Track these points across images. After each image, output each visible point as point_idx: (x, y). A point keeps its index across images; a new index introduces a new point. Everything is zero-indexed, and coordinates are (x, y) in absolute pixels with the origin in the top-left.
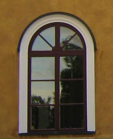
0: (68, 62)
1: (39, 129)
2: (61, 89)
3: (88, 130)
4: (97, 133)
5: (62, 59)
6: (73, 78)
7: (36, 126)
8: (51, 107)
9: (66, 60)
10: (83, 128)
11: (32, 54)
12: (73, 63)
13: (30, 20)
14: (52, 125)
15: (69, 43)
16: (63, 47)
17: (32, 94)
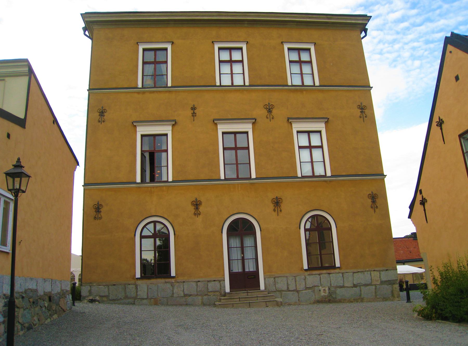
0: (160, 241)
1: (146, 276)
2: (157, 255)
3: (171, 276)
4: (176, 277)
5: (157, 239)
6: (163, 249)
7: (145, 274)
8: (153, 264)
9: (160, 240)
10: (169, 275)
11: (142, 237)
12: (163, 241)
13: (141, 220)
14: (153, 273)
15: (161, 231)
16: (158, 233)
17: (142, 258)
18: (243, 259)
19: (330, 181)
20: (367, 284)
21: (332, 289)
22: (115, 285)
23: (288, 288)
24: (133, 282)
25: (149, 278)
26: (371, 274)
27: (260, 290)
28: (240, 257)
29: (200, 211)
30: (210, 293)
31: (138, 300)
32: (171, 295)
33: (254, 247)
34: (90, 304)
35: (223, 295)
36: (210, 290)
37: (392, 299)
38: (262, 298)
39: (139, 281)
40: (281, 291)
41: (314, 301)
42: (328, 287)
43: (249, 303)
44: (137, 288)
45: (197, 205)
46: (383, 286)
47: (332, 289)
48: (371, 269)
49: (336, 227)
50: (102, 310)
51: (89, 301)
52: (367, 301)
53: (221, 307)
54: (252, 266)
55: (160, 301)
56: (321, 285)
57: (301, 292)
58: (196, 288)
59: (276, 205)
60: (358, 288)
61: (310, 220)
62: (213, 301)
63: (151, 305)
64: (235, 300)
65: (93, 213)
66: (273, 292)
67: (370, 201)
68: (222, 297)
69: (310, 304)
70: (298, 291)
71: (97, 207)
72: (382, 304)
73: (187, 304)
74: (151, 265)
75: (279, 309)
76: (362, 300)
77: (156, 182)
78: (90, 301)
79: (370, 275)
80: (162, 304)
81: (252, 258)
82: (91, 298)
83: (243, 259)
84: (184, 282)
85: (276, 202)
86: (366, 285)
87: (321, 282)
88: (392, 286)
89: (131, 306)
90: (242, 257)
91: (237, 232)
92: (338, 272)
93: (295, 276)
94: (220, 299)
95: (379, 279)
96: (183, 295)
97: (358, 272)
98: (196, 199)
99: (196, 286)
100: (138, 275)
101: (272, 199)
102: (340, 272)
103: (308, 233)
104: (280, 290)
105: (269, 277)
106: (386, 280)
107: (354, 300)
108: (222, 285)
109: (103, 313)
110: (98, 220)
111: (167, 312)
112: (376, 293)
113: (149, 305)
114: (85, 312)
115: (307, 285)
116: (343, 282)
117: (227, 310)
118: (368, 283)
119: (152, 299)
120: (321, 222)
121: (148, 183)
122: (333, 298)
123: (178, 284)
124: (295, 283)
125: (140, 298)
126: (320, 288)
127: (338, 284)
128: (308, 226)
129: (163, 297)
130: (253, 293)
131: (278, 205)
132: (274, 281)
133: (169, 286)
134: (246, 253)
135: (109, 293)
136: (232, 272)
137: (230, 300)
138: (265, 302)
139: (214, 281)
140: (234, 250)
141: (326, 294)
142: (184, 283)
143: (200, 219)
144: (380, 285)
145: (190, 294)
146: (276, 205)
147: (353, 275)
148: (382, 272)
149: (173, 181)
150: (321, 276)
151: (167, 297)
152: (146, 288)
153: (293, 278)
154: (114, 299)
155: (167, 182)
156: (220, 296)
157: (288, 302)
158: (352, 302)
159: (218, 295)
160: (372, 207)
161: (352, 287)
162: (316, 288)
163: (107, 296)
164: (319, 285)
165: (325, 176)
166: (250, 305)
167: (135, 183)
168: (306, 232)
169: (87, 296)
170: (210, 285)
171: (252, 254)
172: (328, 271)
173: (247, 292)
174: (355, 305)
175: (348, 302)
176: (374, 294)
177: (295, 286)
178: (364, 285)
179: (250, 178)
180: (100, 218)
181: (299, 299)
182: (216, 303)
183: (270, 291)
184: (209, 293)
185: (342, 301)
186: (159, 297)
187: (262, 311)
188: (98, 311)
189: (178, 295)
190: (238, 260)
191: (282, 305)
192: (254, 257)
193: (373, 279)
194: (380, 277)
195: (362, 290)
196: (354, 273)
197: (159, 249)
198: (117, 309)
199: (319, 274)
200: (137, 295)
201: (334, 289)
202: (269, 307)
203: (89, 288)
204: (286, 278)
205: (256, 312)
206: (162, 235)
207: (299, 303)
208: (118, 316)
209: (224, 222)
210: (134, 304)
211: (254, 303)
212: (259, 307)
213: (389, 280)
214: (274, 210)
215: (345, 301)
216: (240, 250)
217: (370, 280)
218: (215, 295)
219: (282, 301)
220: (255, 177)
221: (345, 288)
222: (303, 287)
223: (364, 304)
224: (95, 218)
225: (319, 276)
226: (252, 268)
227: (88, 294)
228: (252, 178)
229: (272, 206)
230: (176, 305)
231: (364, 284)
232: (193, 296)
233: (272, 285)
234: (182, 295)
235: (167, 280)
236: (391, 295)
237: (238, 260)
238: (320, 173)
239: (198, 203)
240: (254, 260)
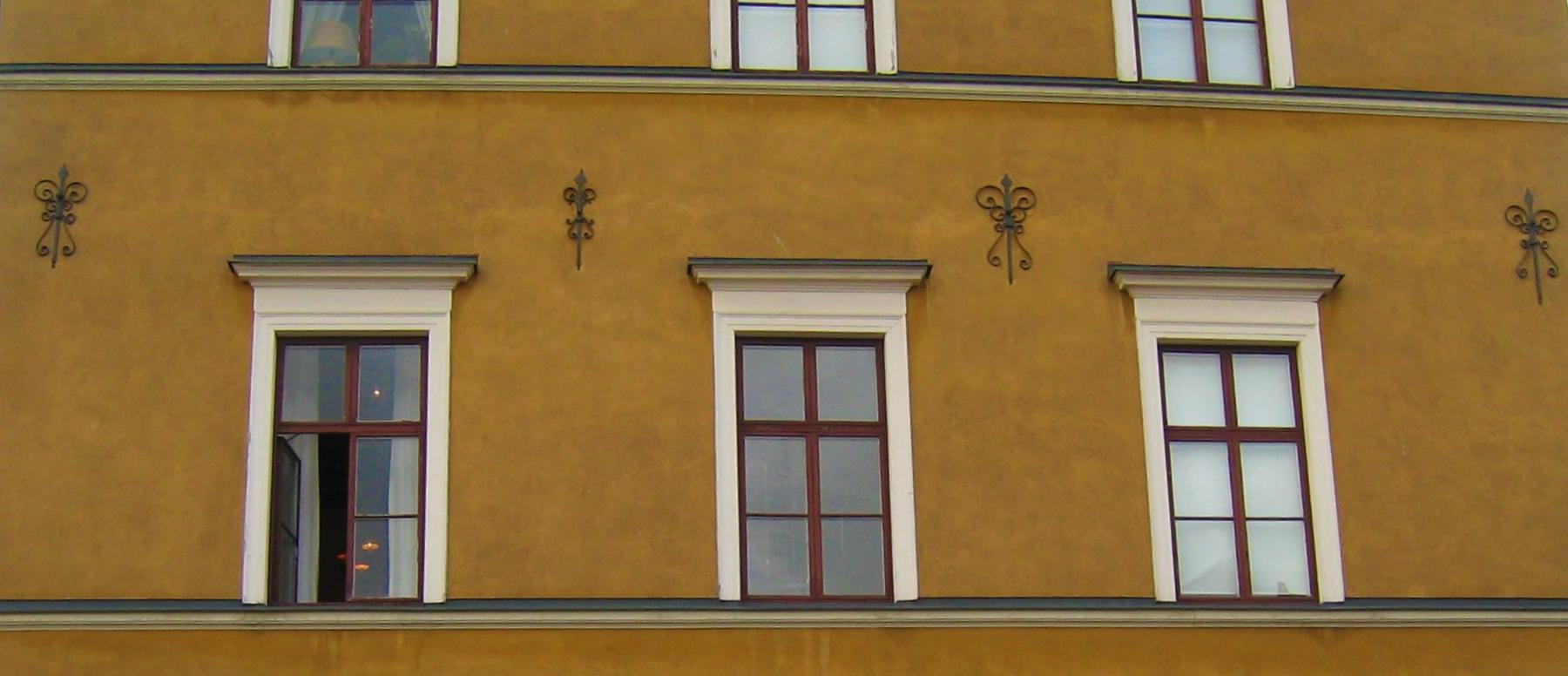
19: (1341, 631)
121: (307, 608)
149: (450, 605)
155: (416, 604)
165: (1310, 602)
179: (886, 600)
220: (915, 597)
228: (896, 600)
238: (1281, 585)
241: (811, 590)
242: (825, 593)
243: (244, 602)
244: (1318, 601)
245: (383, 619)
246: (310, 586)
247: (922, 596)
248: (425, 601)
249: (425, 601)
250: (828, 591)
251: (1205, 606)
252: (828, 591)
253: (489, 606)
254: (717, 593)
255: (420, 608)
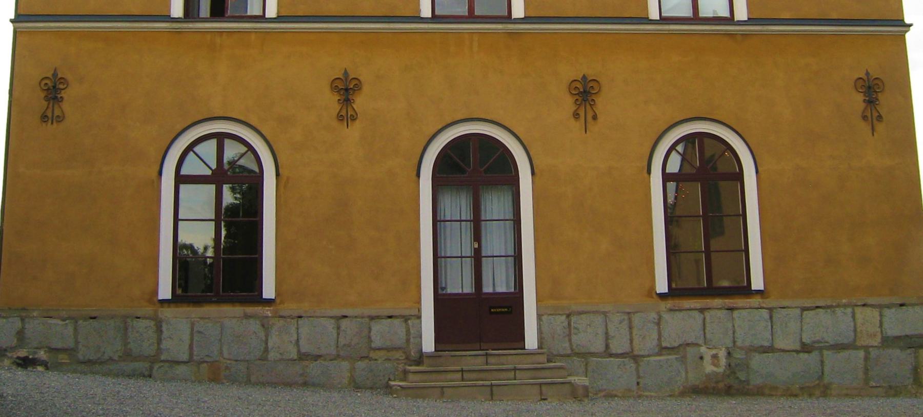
0: (235, 193)
1: (189, 294)
2: (224, 233)
3: (264, 297)
4: (278, 301)
5: (226, 188)
6: (243, 217)
7: (185, 290)
9: (233, 190)
10: (256, 293)
11: (181, 179)
12: (243, 194)
13: (179, 128)
14: (209, 288)
15: (238, 163)
16: (228, 170)
17: (179, 240)
18: (477, 257)
19: (745, 35)
20: (841, 344)
21: (739, 355)
22: (94, 318)
23: (607, 346)
24: (149, 310)
25: (197, 301)
26: (853, 316)
27: (524, 348)
28: (468, 251)
29: (354, 109)
30: (377, 351)
31: (162, 366)
32: (261, 354)
33: (512, 222)
34: (20, 373)
35: (415, 361)
36: (377, 342)
37: (914, 391)
38: (529, 374)
39: (167, 309)
40: (585, 355)
41: (681, 388)
42: (727, 348)
43: (489, 389)
44: (159, 330)
45: (347, 90)
46: (890, 351)
47: (739, 355)
48: (855, 301)
49: (757, 172)
50: (55, 392)
51: (18, 361)
52: (839, 396)
53: (407, 396)
54: (504, 278)
55: (227, 371)
56: (705, 343)
57: (645, 359)
58: (335, 335)
59: (580, 99)
60: (815, 355)
61: (680, 148)
62: (384, 376)
63: (199, 382)
64: (449, 376)
65: (39, 102)
66: (562, 356)
67: (860, 98)
68: (410, 365)
69: (670, 396)
70: (636, 358)
71: (53, 85)
72: (885, 404)
73: (305, 384)
74: (205, 262)
75: (577, 408)
76: (825, 391)
77: (229, 17)
78: (20, 362)
79: (852, 319)
80: (233, 380)
81: (503, 254)
82: (23, 353)
83: (477, 257)
84: (300, 317)
85: (582, 90)
86: (838, 347)
87: (705, 334)
88: (915, 353)
89: (141, 382)
90: (475, 249)
91: (462, 175)
92: (757, 306)
93: (629, 313)
94: (405, 372)
95: (879, 330)
96: (296, 357)
97: (817, 307)
98: (346, 73)
99: (335, 332)
100: (165, 291)
101: (572, 79)
102: (764, 305)
103: (672, 186)
104: (583, 351)
105: (552, 313)
106: (899, 335)
107: (802, 389)
108: (412, 332)
109: (56, 398)
110: (52, 123)
111: (246, 403)
112: (866, 371)
113: (192, 382)
114: (5, 395)
115: (663, 339)
116: (772, 335)
117: (425, 405)
118: (845, 341)
119: (205, 365)
120: (713, 156)
121: (205, 20)
122: (741, 381)
123: (282, 322)
124: (628, 333)
125: (170, 359)
126: (703, 349)
127: (755, 342)
128: (674, 166)
129: (236, 361)
130: (506, 359)
131: (588, 100)
132: (566, 324)
133: (254, 326)
134: (488, 240)
135: (77, 342)
136: (444, 292)
137: (434, 376)
138: (537, 387)
139: (390, 317)
140: (451, 229)
141: (720, 370)
142: (301, 321)
143: (354, 132)
144: (881, 350)
145: (318, 354)
146: (580, 99)
147: (802, 316)
148: (887, 312)
149: (279, 19)
150: (708, 314)
151: (247, 361)
152: (188, 331)
153: (622, 318)
154: (91, 358)
155: (262, 18)
156: (405, 364)
157: (605, 387)
158: (796, 396)
159: (398, 359)
160: (864, 118)
161: (797, 352)
162: (690, 350)
163: (72, 349)
164: (701, 342)
165: (730, 20)
166: (492, 393)
167: (168, 18)
168: (668, 184)
169: (13, 349)
170: (378, 328)
171: (506, 242)
172: (729, 302)
173: (487, 354)
174: (803, 404)
175: (784, 395)
176: (861, 375)
177: (629, 342)
178: (831, 345)
179: (508, 18)
180: (60, 119)
181: (639, 380)
182: (392, 383)
183: (555, 353)
184: (372, 352)
185: (767, 391)
186: (224, 359)
187: (528, 411)
188: (43, 394)
189: (281, 354)
190: (461, 257)
191: (587, 396)
192: (511, 252)
193: (861, 330)
194: (881, 325)
195: (826, 362)
196: (804, 309)
197: (230, 216)
198: (100, 390)
199: (702, 310)
200: (159, 351)
201: (744, 356)
202: (549, 400)
203: (18, 324)
204: (603, 316)
205: (511, 413)
206: (241, 174)
207: (637, 392)
208: (103, 409)
209: (424, 144)
210: (150, 376)
211: (506, 388)
212: (520, 400)
213: (907, 336)
214: (576, 115)
215: (774, 393)
216: (469, 230)
217: (852, 334)
218: (390, 360)
219: (587, 384)
220: (523, 16)
221: (777, 354)
222: (652, 347)
223: (832, 404)
224: (44, 118)
225: (702, 316)
226: (504, 285)
227: (15, 341)
228: (513, 18)
229: (569, 103)
230: (274, 385)
231: (831, 343)
232: (325, 360)
233: (559, 335)
234: (294, 355)
235: (250, 310)
236: (911, 380)
237: (461, 257)
238: (714, 12)
239: (352, 87)
240: (511, 260)
241: (468, 12)
242: (476, 14)
243: (172, 16)
244: (734, 20)
245: (244, 26)
246: (206, 9)
247: (526, 16)
248: (266, 17)
249: (266, 17)
250: (477, 12)
251: (676, 22)
252: (477, 12)
253: (300, 19)
254: (419, 14)
255: (264, 20)
